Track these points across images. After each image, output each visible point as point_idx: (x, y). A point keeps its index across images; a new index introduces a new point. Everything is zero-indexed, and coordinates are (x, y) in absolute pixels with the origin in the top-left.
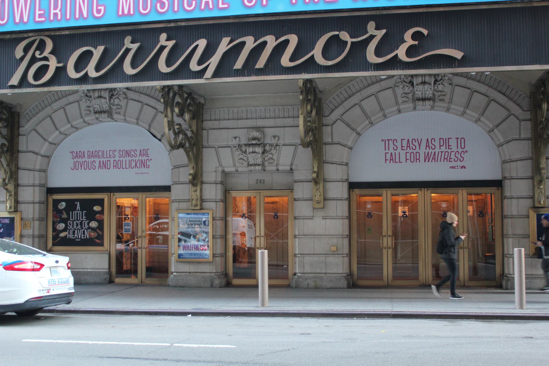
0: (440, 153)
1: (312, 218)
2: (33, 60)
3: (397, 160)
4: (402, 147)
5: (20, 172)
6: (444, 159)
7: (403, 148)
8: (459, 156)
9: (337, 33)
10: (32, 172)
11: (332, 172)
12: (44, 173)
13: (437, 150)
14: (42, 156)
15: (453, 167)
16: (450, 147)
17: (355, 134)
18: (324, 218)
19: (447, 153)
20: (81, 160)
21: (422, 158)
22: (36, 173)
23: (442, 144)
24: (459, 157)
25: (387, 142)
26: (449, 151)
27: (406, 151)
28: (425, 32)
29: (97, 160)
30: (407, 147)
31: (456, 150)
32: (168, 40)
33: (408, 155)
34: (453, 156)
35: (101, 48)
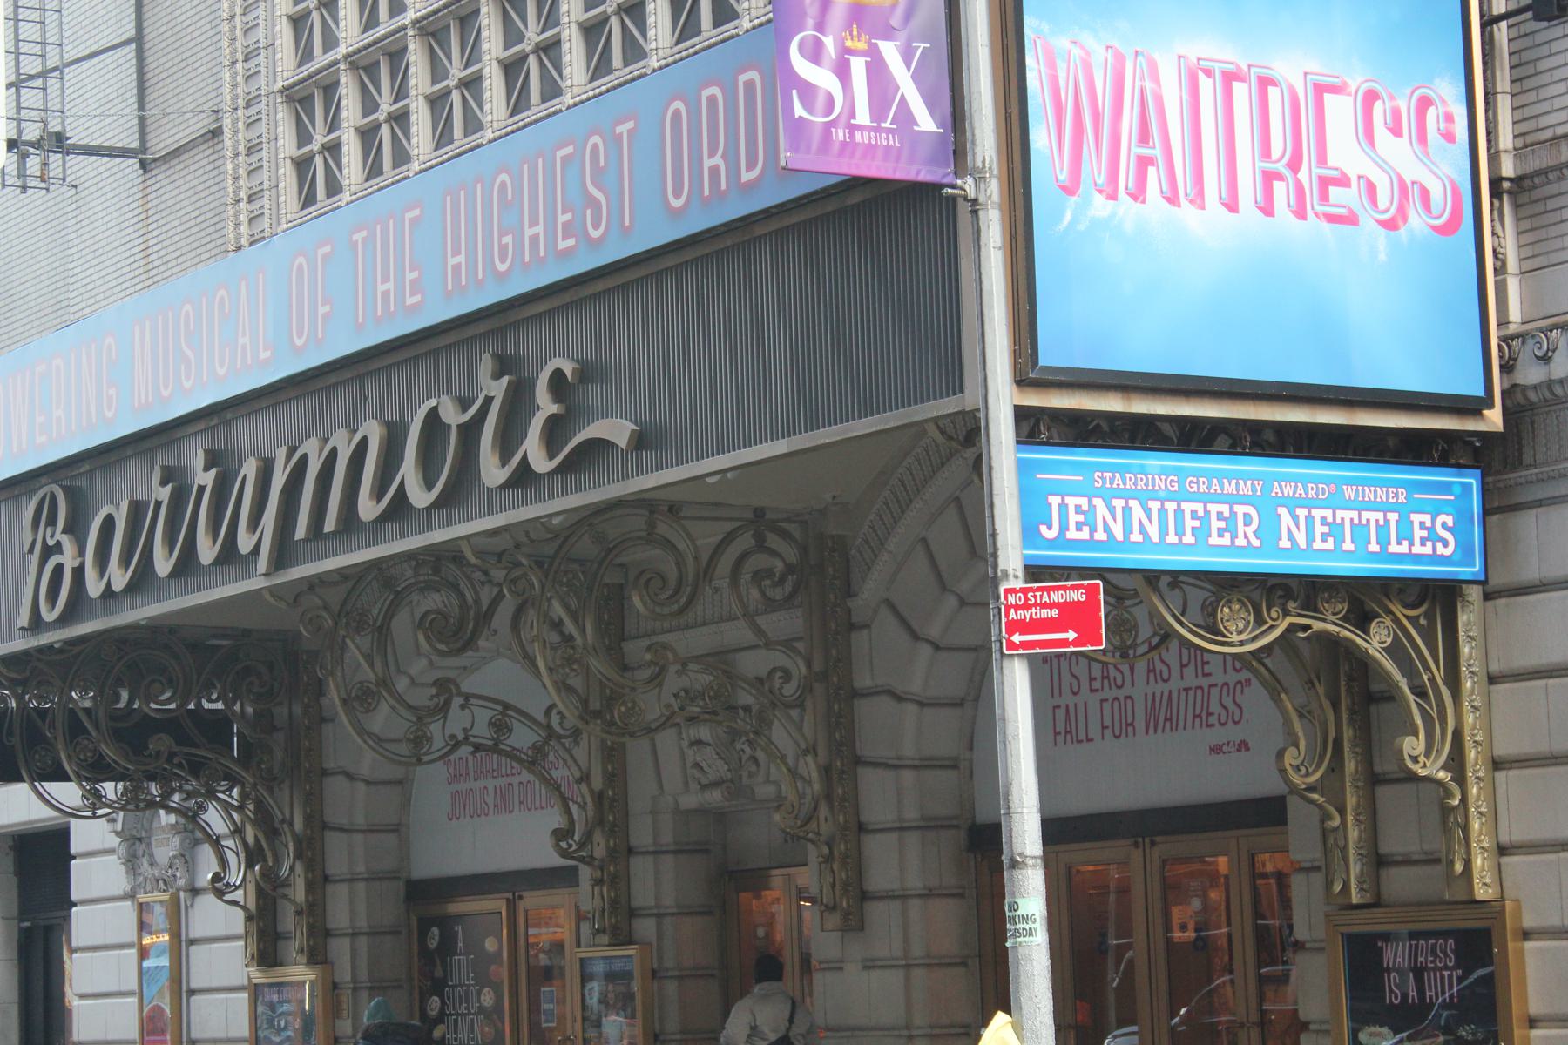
0: (1183, 695)
1: (837, 967)
2: (48, 552)
3: (1082, 736)
4: (1092, 679)
5: (328, 834)
6: (1195, 716)
7: (1097, 685)
8: (1228, 702)
9: (433, 402)
10: (344, 836)
11: (880, 797)
12: (390, 840)
13: (1175, 684)
14: (368, 783)
15: (1216, 749)
16: (1207, 669)
17: (925, 650)
18: (869, 965)
19: (1199, 692)
20: (463, 787)
21: (1140, 724)
22: (358, 838)
23: (1185, 661)
24: (1231, 707)
25: (1055, 661)
26: (1205, 682)
27: (1100, 696)
28: (568, 368)
29: (491, 784)
30: (1103, 678)
31: (1220, 682)
32: (206, 469)
33: (1107, 706)
34: (1215, 707)
35: (124, 505)
